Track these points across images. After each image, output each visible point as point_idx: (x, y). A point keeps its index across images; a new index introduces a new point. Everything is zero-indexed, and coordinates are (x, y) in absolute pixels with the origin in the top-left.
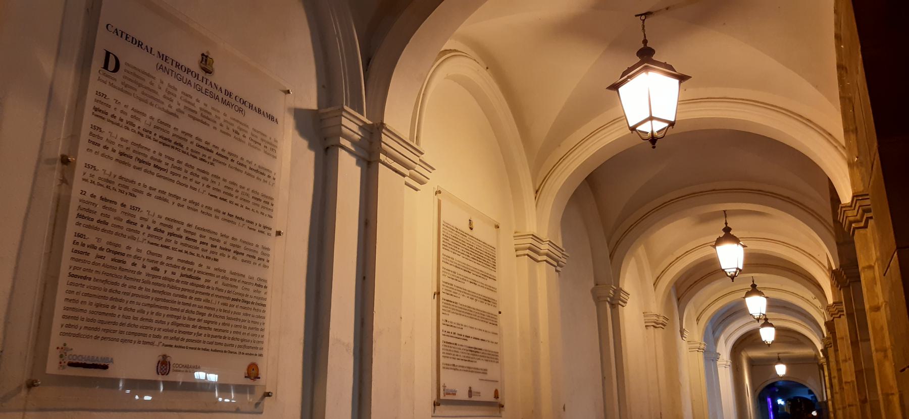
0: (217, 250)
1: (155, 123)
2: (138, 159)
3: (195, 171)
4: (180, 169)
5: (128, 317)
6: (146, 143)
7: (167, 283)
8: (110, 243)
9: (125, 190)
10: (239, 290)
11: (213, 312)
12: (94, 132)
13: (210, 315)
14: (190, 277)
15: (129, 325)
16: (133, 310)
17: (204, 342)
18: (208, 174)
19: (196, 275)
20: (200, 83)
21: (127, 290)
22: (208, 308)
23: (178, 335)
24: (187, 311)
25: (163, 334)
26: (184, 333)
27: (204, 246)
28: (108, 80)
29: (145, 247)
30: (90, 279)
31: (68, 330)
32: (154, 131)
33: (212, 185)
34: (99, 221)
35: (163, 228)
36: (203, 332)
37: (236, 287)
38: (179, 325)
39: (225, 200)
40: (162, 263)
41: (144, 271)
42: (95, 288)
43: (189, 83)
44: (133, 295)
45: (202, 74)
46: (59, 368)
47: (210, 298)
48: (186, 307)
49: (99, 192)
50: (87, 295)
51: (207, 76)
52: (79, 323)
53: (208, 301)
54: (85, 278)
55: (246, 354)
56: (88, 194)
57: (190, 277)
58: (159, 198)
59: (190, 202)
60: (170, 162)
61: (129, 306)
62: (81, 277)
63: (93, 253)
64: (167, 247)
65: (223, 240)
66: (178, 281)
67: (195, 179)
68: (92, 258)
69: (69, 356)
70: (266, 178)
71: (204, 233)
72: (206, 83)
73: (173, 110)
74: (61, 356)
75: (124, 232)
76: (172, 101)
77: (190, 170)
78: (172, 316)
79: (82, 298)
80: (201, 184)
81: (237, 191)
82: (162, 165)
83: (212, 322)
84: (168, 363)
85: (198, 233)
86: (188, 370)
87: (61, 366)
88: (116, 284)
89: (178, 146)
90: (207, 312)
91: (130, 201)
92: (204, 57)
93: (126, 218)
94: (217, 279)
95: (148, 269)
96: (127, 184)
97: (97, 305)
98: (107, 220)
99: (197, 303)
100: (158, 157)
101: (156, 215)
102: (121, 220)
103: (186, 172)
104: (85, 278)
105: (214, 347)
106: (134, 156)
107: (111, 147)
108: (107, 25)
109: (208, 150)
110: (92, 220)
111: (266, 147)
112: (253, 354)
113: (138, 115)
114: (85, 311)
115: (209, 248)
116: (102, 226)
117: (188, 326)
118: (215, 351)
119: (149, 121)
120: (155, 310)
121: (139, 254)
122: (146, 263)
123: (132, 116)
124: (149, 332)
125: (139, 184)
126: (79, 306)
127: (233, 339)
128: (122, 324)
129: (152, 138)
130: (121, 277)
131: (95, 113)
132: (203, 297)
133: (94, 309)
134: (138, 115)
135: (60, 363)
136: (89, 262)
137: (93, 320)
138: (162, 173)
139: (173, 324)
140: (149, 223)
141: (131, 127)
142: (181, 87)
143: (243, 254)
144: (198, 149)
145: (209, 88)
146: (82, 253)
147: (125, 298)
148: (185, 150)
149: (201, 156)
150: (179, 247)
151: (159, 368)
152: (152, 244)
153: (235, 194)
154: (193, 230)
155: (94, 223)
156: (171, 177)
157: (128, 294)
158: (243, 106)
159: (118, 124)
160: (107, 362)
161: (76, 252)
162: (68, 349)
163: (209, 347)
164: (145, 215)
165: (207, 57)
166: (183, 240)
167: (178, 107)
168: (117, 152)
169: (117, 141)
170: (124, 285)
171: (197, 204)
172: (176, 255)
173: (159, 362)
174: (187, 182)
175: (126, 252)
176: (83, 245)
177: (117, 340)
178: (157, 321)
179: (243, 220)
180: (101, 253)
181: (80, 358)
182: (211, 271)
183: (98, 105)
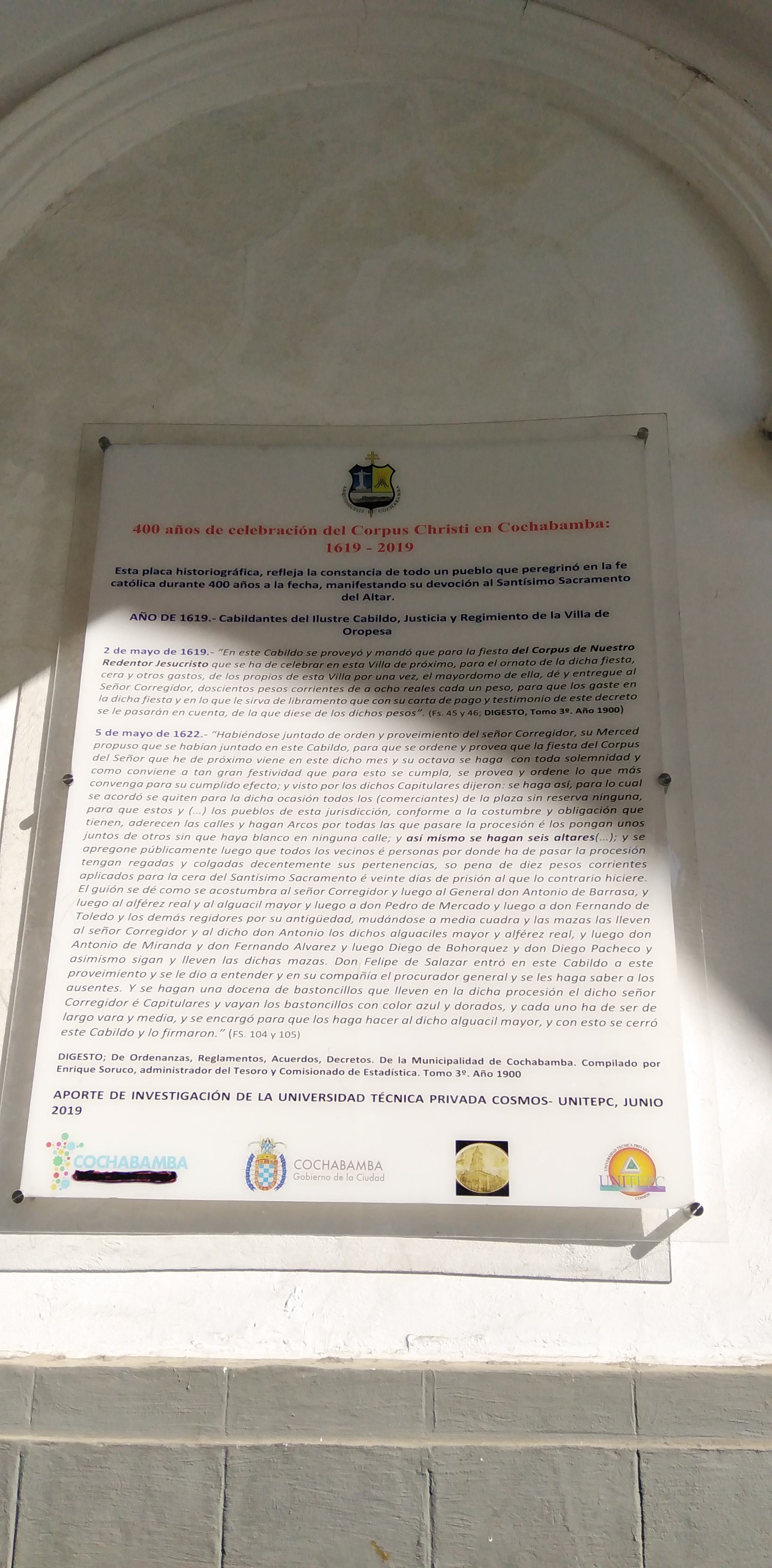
46: (54, 1187)
74: (58, 1161)
86: (342, 1173)
87: (58, 1181)
135: (56, 1175)
162: (72, 1146)
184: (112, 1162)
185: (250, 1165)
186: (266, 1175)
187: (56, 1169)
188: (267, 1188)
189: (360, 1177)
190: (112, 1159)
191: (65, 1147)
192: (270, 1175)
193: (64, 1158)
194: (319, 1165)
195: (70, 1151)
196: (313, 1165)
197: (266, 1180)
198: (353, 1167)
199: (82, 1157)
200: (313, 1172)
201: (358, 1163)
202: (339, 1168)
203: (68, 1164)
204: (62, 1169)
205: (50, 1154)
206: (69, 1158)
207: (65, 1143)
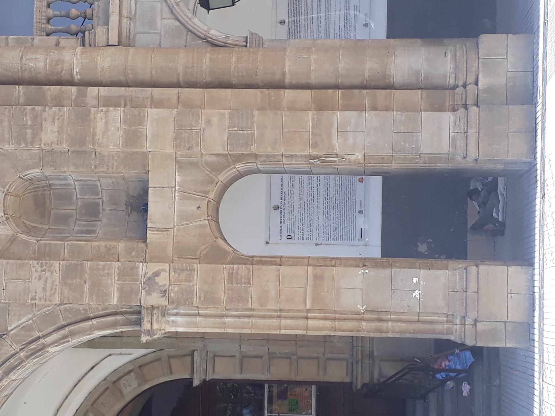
1: (299, 223)
4: (309, 213)
6: (306, 225)
27: (328, 202)
29: (332, 221)
45: (280, 209)
48: (345, 206)
51: (280, 207)
57: (337, 206)
59: (317, 208)
67: (310, 208)
71: (325, 203)
77: (309, 210)
91: (322, 228)
106: (310, 228)
107: (310, 235)
122: (336, 220)
138: (312, 219)
142: (287, 216)
144: (302, 208)
153: (311, 193)
156: (312, 216)
158: (283, 192)
164: (324, 223)
165: (274, 208)
169: (308, 233)
171: (317, 206)
172: (332, 211)
175: (334, 227)
180: (336, 233)
183: (301, 239)
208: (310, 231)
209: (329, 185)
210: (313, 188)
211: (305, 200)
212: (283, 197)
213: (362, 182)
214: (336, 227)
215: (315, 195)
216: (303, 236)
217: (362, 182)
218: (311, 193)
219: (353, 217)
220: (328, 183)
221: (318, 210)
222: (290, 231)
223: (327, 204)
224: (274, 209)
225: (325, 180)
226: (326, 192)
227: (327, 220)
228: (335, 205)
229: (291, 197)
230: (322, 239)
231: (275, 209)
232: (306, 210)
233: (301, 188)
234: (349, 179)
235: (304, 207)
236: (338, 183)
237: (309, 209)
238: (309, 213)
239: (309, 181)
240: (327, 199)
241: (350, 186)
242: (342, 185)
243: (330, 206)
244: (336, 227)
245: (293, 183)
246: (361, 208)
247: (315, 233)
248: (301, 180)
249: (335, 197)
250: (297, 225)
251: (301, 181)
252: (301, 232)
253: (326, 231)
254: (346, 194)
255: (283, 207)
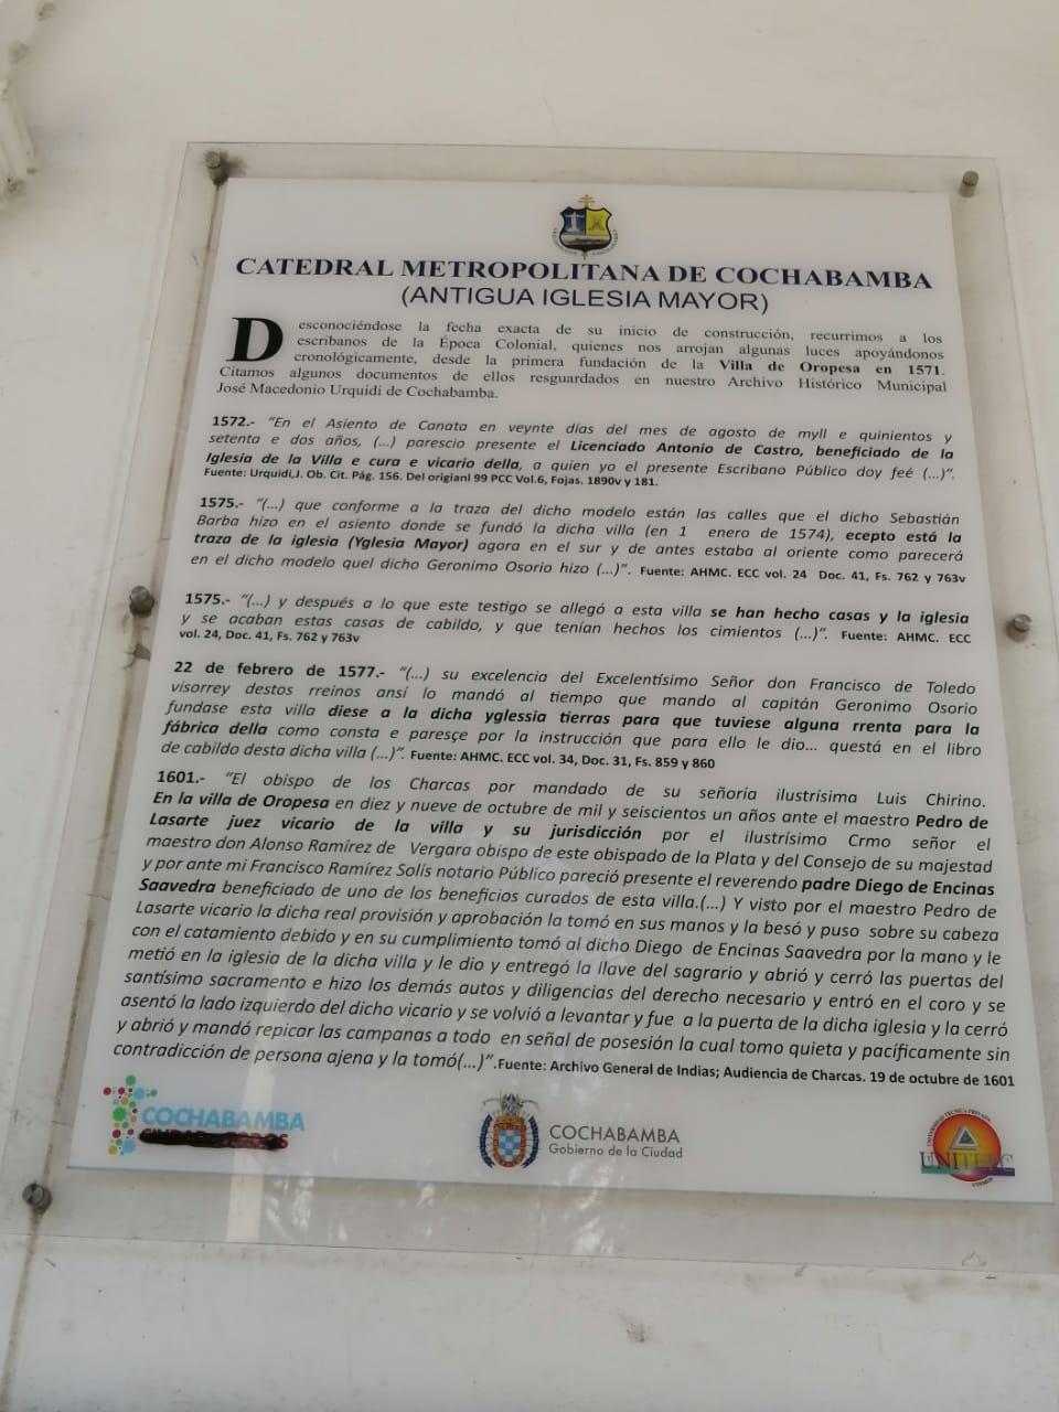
0: (707, 729)
2: (358, 542)
3: (575, 519)
4: (512, 528)
5: (355, 985)
6: (378, 491)
7: (496, 863)
8: (276, 780)
9: (322, 631)
10: (837, 847)
11: (713, 939)
12: (210, 512)
13: (701, 949)
14: (593, 832)
15: (357, 1009)
16: (373, 962)
17: (687, 1046)
18: (630, 513)
19: (618, 822)
20: (570, 285)
21: (342, 902)
22: (692, 926)
23: (559, 1028)
24: (594, 945)
25: (497, 1028)
26: (591, 1017)
27: (646, 731)
28: (248, 380)
29: (402, 771)
30: (211, 888)
31: (140, 1038)
32: (405, 455)
33: (652, 543)
34: (237, 729)
35: (464, 706)
36: (678, 1009)
37: (821, 841)
38: (559, 994)
39: (719, 572)
40: (472, 807)
41: (402, 842)
42: (227, 911)
43: (526, 296)
44: (367, 916)
45: (567, 259)
46: (112, 1151)
47: (693, 891)
48: (588, 933)
49: (230, 653)
50: (199, 933)
51: (593, 257)
52: (179, 1015)
53: (681, 901)
54: (195, 887)
55: (914, 1079)
56: (199, 668)
57: (593, 832)
58: (446, 625)
59: (565, 609)
60: (476, 521)
61: (353, 949)
62: (182, 887)
63: (219, 816)
64: (490, 757)
65: (725, 696)
66: (542, 852)
68: (217, 826)
69: (144, 1114)
70: (904, 461)
72: (590, 277)
73: (474, 382)
74: (119, 1114)
75: (323, 741)
76: (463, 361)
77: (553, 521)
78: (528, 966)
79: (181, 944)
80: (605, 550)
81: (768, 534)
82: (448, 535)
83: (717, 974)
84: (528, 1125)
85: (611, 693)
86: (620, 1145)
87: (119, 1142)
88: (304, 890)
89: (501, 469)
90: (688, 939)
91: (332, 656)
92: (574, 217)
93: (323, 704)
94: (717, 826)
95: (420, 831)
96: (326, 613)
97: (237, 960)
98: (262, 720)
99: (639, 913)
100: (430, 518)
101: (436, 674)
102: (309, 711)
103: (540, 529)
104: (195, 887)
105: (738, 1061)
107: (263, 533)
108: (239, 267)
109: (622, 448)
110: (214, 729)
111: (888, 370)
112: (955, 1080)
113: (346, 433)
114: (196, 980)
115: (666, 731)
116: (243, 740)
117: (599, 993)
118: (747, 1073)
119: (386, 435)
120: (458, 953)
121: (379, 795)
122: (404, 817)
123: (330, 441)
124: (435, 1024)
125: (368, 604)
126: (175, 966)
127: (831, 1025)
128: (330, 1008)
129: (403, 475)
130: (319, 869)
131: (214, 468)
132: (661, 892)
133: (225, 968)
134: (346, 433)
135: (117, 1134)
136: (206, 844)
137: (224, 1004)
138: (447, 556)
139: (534, 991)
140: (414, 699)
141: (326, 469)
142: (491, 318)
143: (835, 726)
144: (581, 457)
145: (607, 285)
146: (182, 821)
147: (340, 927)
148: (527, 471)
149: (594, 472)
150: (534, 747)
151: (489, 1141)
152: (428, 756)
154: (588, 687)
155: (223, 736)
156: (485, 557)
157: (348, 915)
158: (758, 288)
159: (286, 474)
160: (278, 1128)
161: (164, 820)
162: (140, 1094)
163: (717, 1061)
164: (394, 680)
165: (582, 212)
166: (553, 725)
167: (489, 369)
168: (287, 540)
169: (290, 513)
170: (331, 891)
171: (592, 611)
172: (524, 779)
173: (488, 1120)
174: (552, 557)
175: (334, 795)
176: (186, 800)
177: (315, 1057)
178: (465, 989)
179: (815, 615)
180: (245, 812)
181: (184, 1117)
182: (690, 800)
183: (218, 449)
184: (196, 1117)
185: (486, 1132)
186: (509, 1146)
187: (117, 1125)
188: (511, 1164)
189: (647, 1152)
190: (197, 1113)
191: (130, 1095)
192: (516, 1146)
193: (128, 1109)
194: (586, 1133)
195: (137, 1101)
196: (577, 1132)
197: (509, 1152)
198: (636, 1137)
199: (153, 1109)
200: (575, 1143)
201: (644, 1133)
202: (616, 1136)
203: (134, 1119)
204: (125, 1125)
205: (108, 1104)
206: (135, 1111)
207: (131, 1090)
208: (309, 530)
209: (864, 737)
210: (813, 566)
211: (674, 490)
212: (695, 288)
213: (942, 1160)
214: (329, 814)
215: (730, 593)
216: (256, 464)
217: (942, 1160)
218: (760, 545)
219: (451, 1025)
220: (897, 728)
221: (555, 616)
222: (329, 350)
223: (617, 713)
224: (567, 212)
225: (920, 698)
226: (779, 705)
227: (425, 707)
228: (608, 801)
229: (711, 361)
230: (201, 652)
231: (575, 217)
232: (552, 495)
233: (809, 447)
234: (963, 982)
235: (583, 475)
236: (901, 844)
237: (562, 529)
238: (512, 528)
239: (902, 530)
240: (689, 712)
241: (879, 991)
242: (878, 898)
243: (595, 751)
244: (329, 814)
245: (868, 376)
246: (578, 1139)
247: (280, 583)
248: (905, 448)
249: (722, 805)
250: (380, 409)
251: (889, 453)
252: (305, 452)
253: (290, 701)
254: (760, 939)
255: (595, 284)
